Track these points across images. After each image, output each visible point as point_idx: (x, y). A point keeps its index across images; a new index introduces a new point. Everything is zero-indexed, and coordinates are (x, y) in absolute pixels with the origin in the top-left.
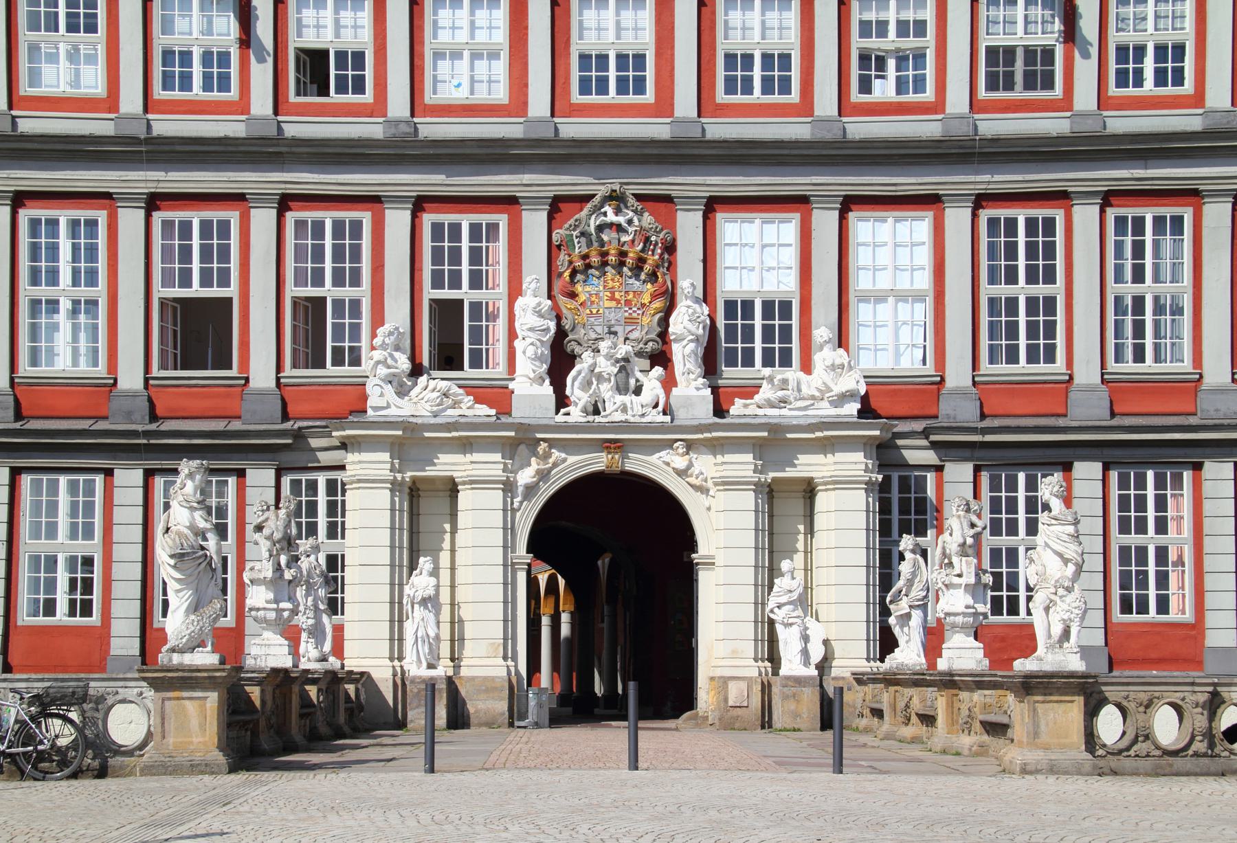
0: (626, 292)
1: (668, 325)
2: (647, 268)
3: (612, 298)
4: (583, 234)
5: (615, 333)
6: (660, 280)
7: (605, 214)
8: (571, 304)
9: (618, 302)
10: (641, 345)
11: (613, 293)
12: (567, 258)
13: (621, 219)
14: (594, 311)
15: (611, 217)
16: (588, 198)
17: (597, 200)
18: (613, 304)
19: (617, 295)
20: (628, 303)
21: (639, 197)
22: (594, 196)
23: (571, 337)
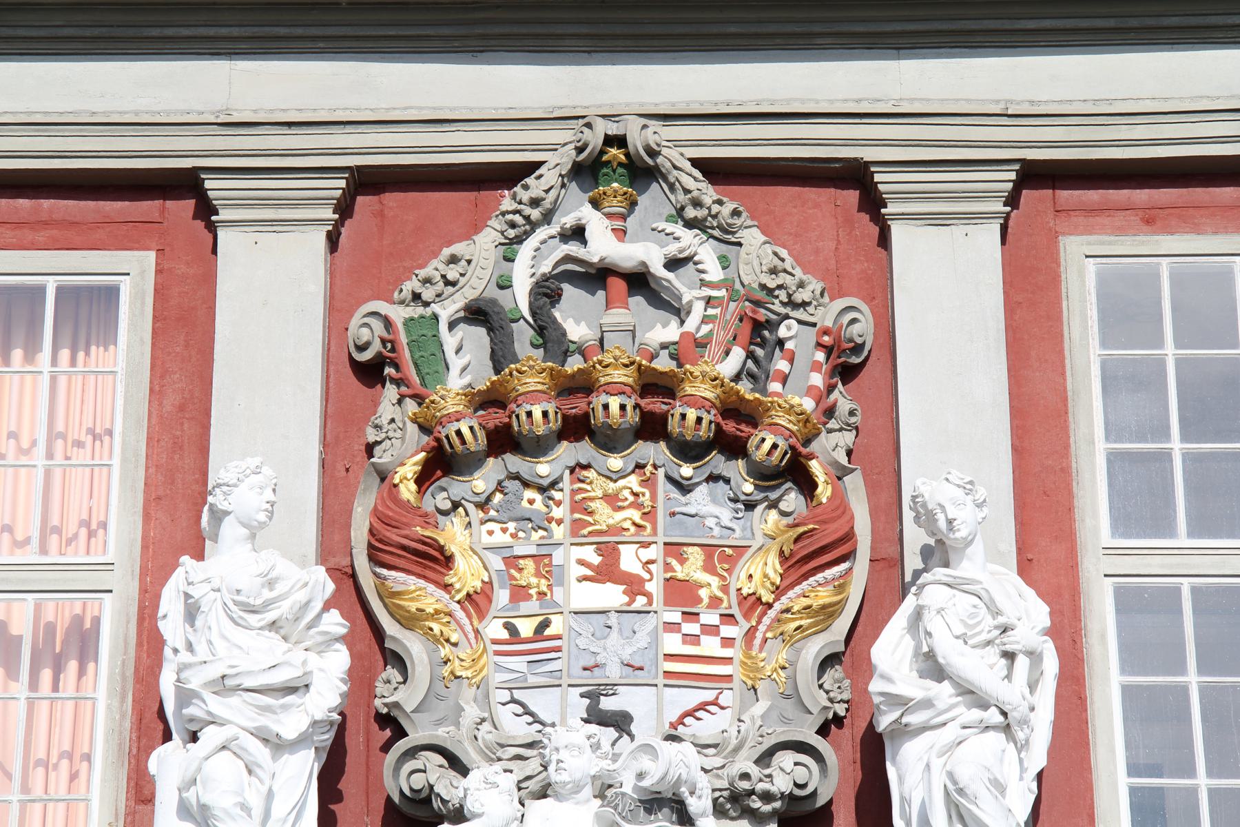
0: (674, 549)
1: (863, 670)
2: (766, 444)
3: (607, 571)
4: (478, 314)
5: (620, 722)
6: (824, 492)
7: (578, 233)
8: (422, 594)
9: (634, 586)
10: (745, 763)
11: (609, 552)
12: (411, 406)
13: (648, 253)
14: (526, 628)
15: (602, 245)
16: (512, 175)
17: (535, 186)
18: (611, 595)
19: (629, 560)
20: (681, 593)
21: (717, 171)
22: (531, 168)
23: (416, 736)
